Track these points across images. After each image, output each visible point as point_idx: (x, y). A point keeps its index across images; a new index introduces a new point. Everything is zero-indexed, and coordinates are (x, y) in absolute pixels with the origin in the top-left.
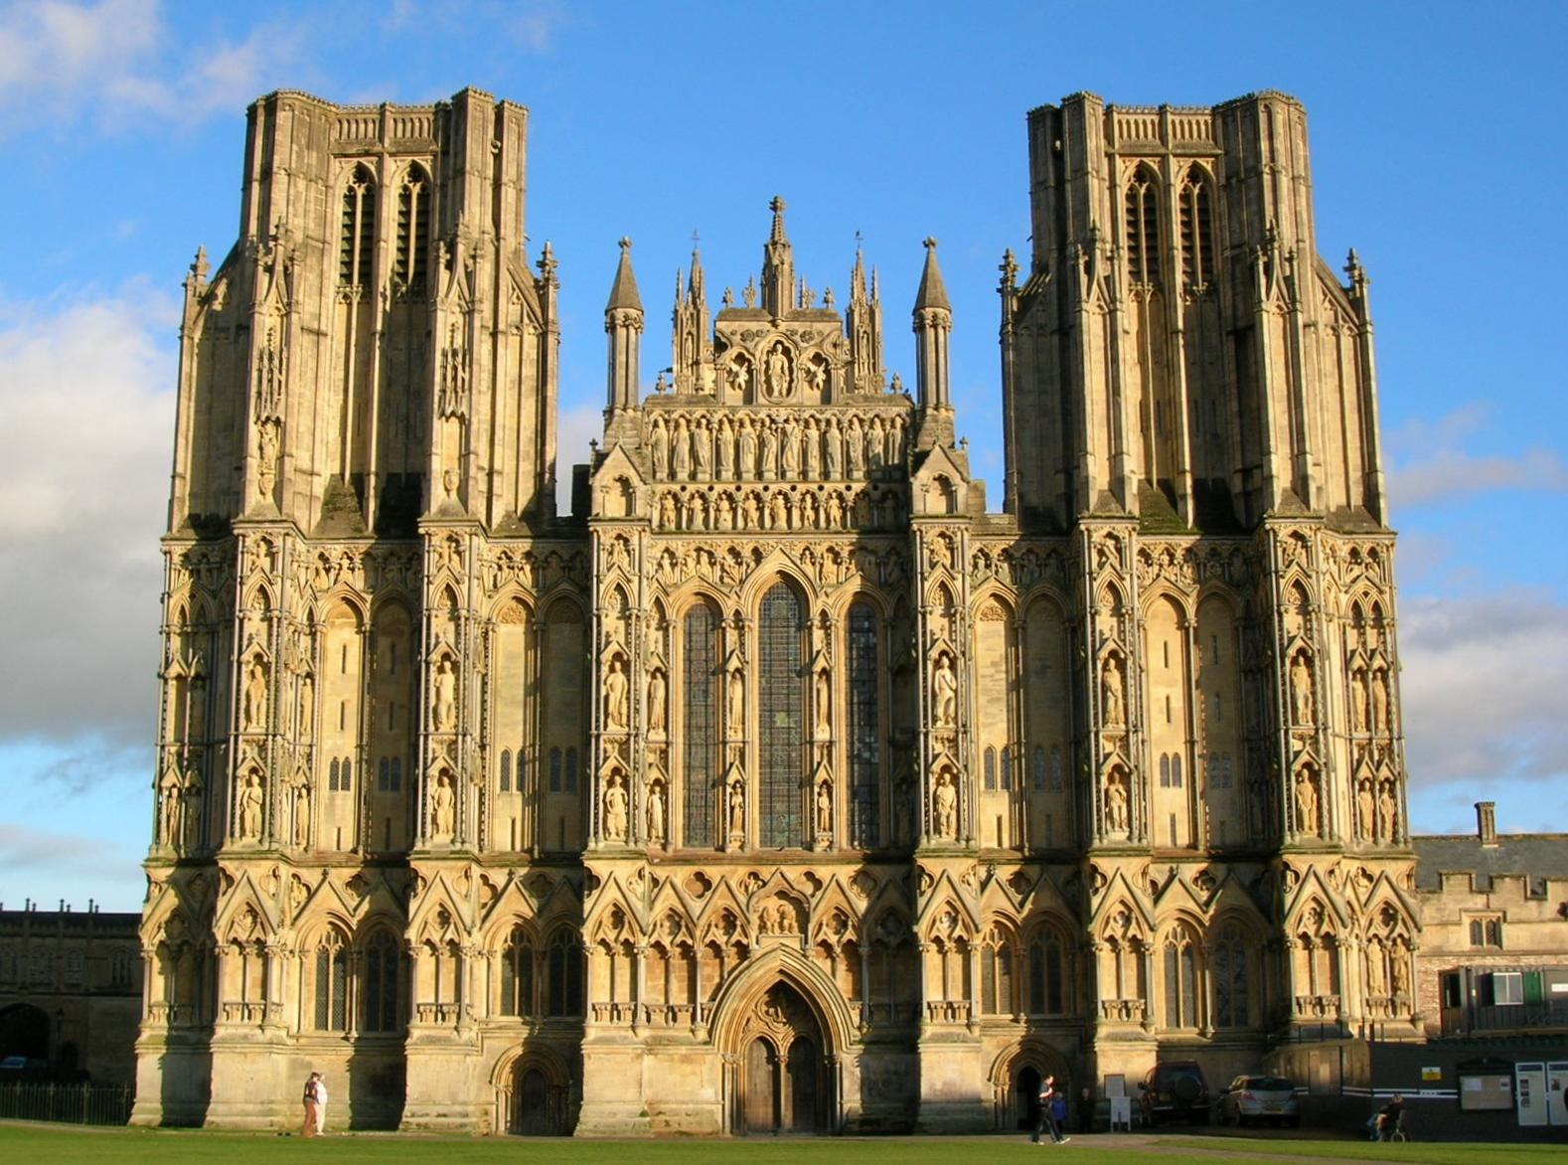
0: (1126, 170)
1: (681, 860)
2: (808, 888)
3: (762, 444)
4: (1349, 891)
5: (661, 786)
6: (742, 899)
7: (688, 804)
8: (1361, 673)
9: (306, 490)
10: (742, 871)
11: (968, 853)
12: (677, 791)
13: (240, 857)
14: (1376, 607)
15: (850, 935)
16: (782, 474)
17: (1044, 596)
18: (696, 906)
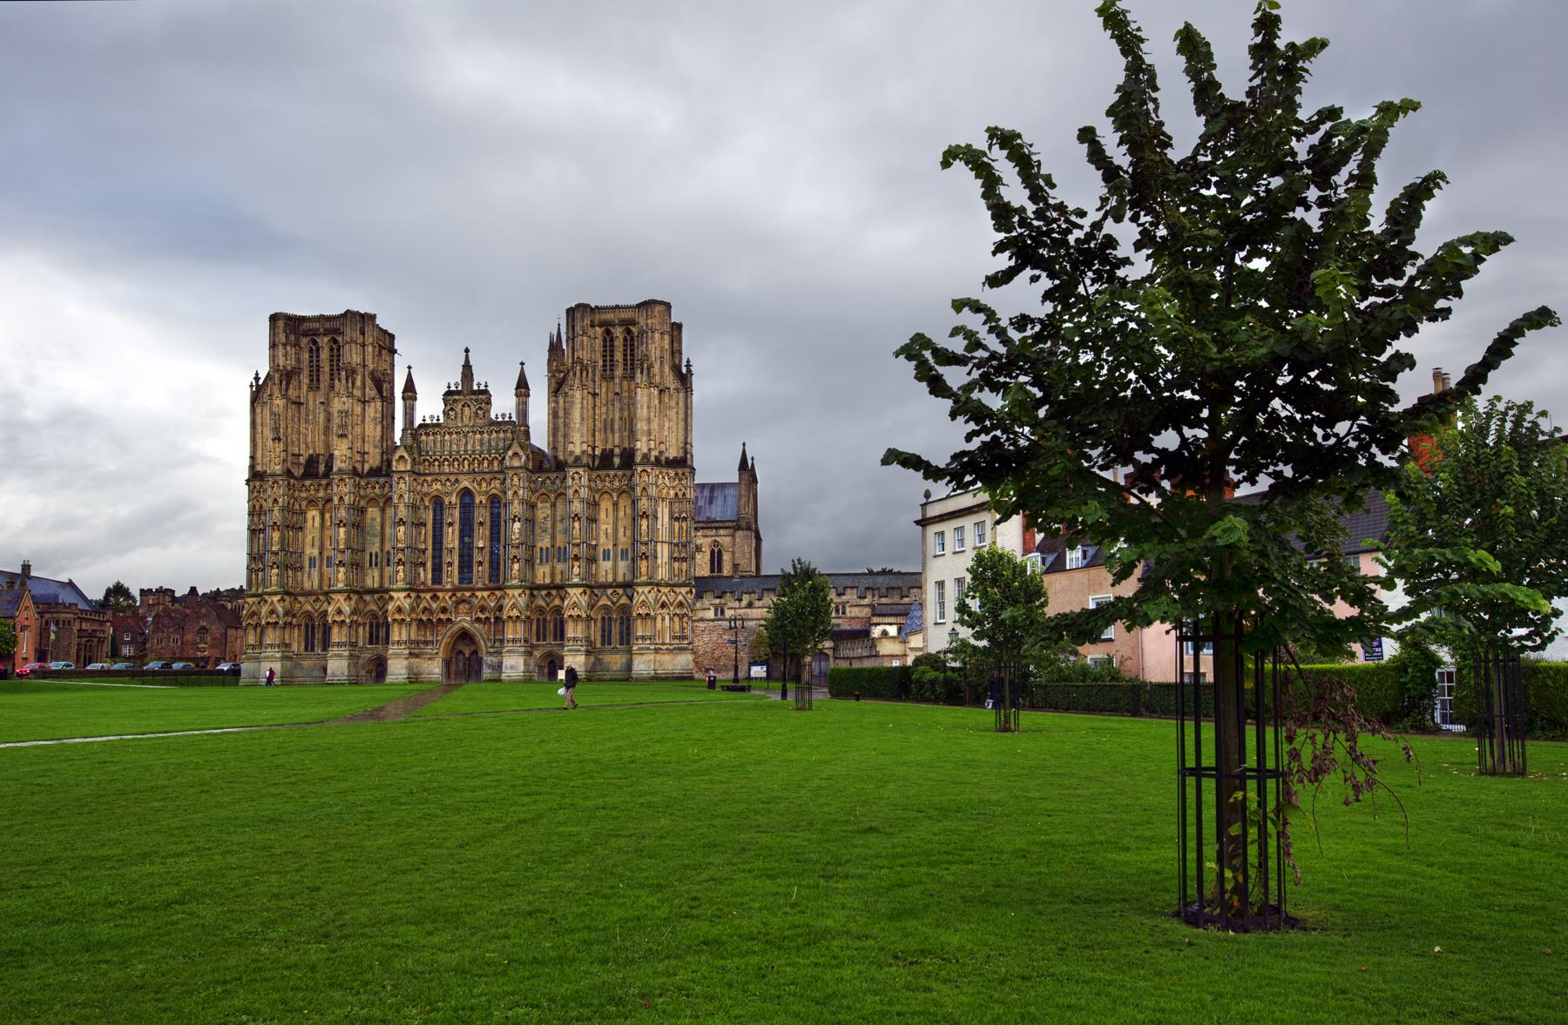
0: (599, 330)
1: (429, 590)
2: (474, 599)
3: (459, 440)
4: (664, 598)
5: (424, 565)
6: (450, 603)
7: (433, 570)
8: (677, 519)
9: (296, 461)
10: (450, 594)
11: (520, 587)
12: (429, 565)
13: (270, 594)
14: (684, 494)
15: (487, 614)
16: (466, 451)
17: (561, 494)
18: (434, 606)
